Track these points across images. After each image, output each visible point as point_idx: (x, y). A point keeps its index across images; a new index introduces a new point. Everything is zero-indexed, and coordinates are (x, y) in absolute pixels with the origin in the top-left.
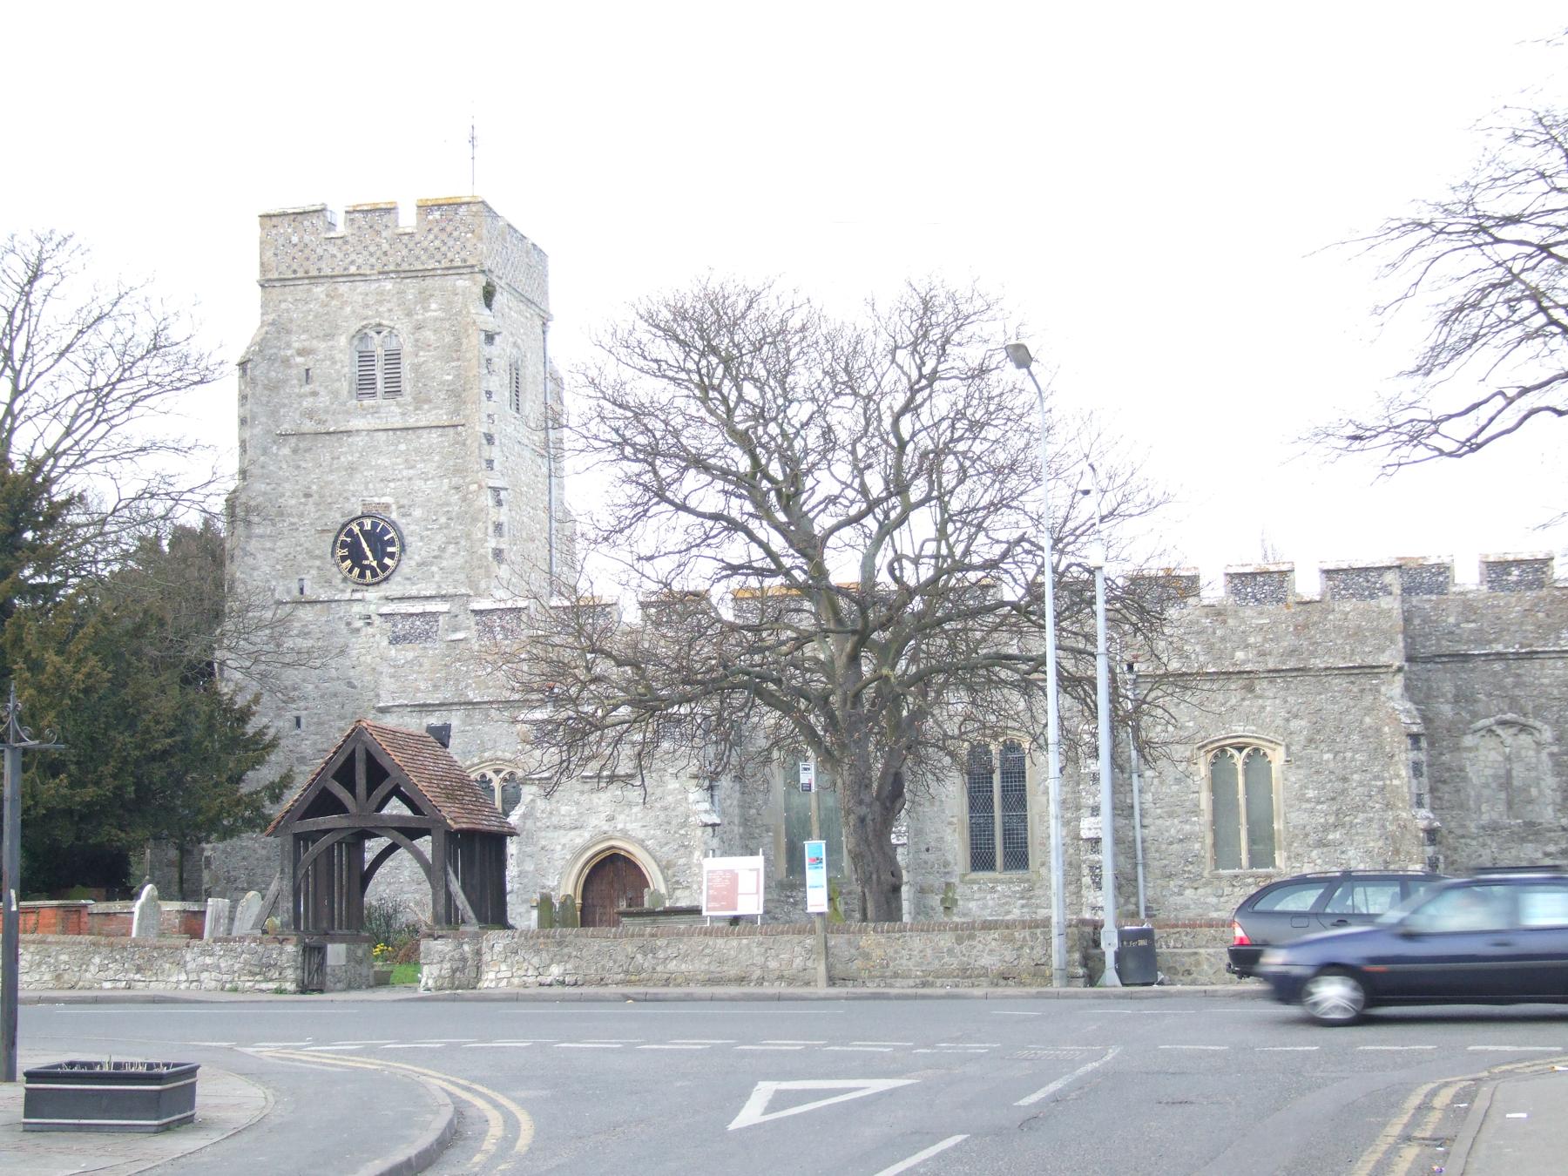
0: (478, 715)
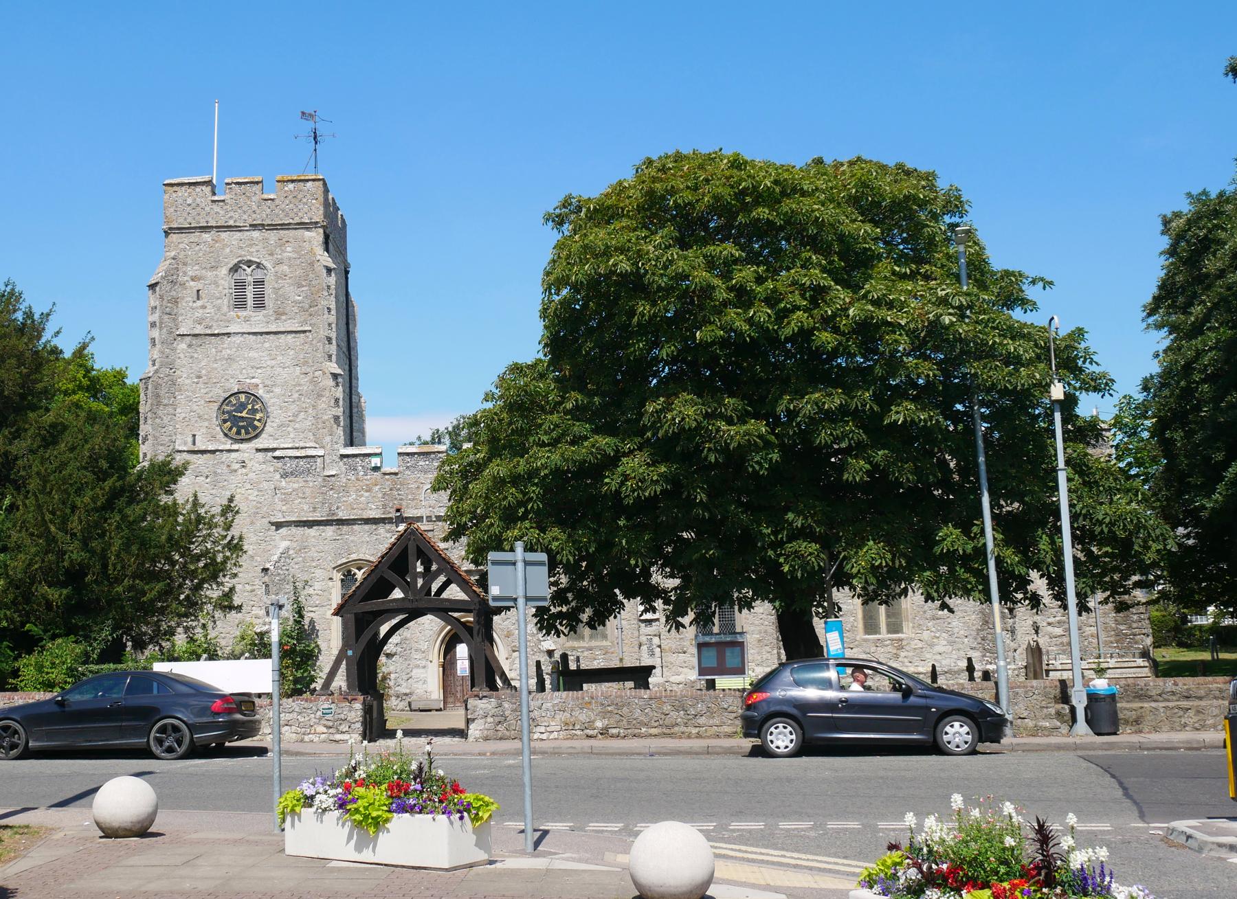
0: (345, 528)
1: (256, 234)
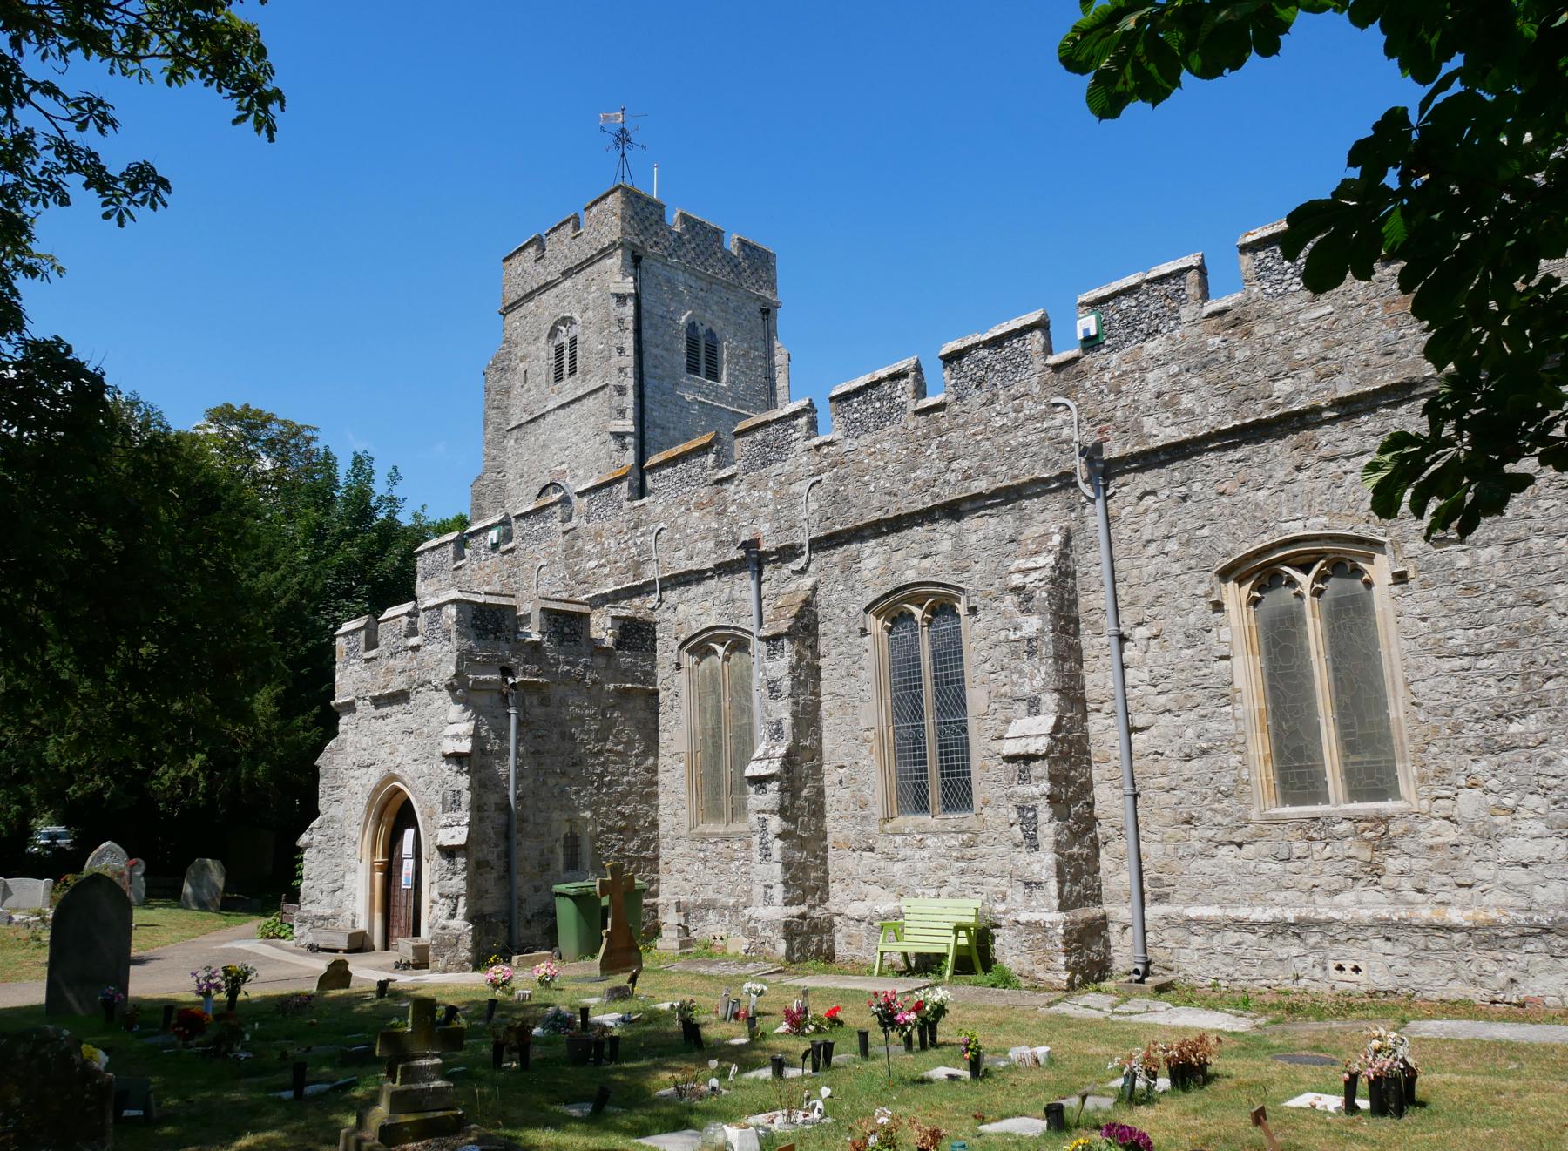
1: (568, 283)
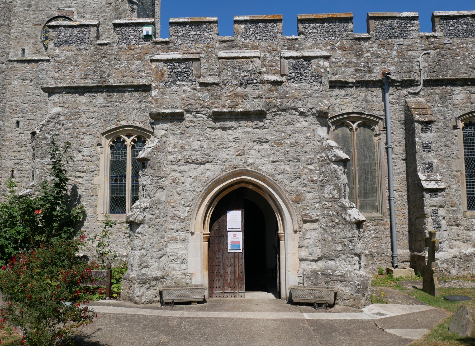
0: (115, 95)
